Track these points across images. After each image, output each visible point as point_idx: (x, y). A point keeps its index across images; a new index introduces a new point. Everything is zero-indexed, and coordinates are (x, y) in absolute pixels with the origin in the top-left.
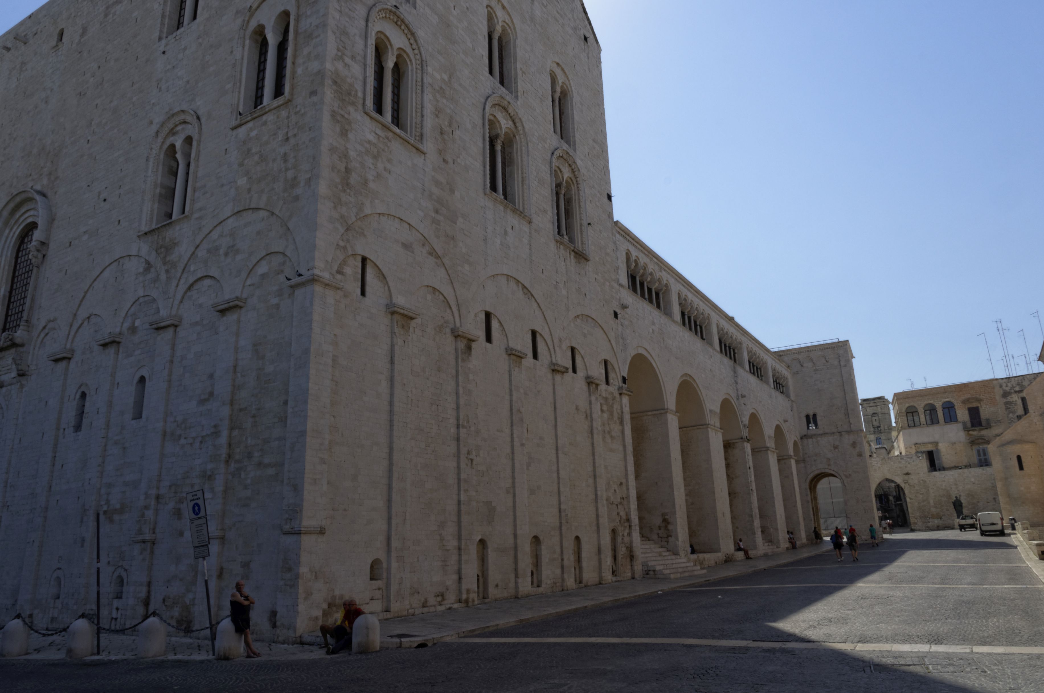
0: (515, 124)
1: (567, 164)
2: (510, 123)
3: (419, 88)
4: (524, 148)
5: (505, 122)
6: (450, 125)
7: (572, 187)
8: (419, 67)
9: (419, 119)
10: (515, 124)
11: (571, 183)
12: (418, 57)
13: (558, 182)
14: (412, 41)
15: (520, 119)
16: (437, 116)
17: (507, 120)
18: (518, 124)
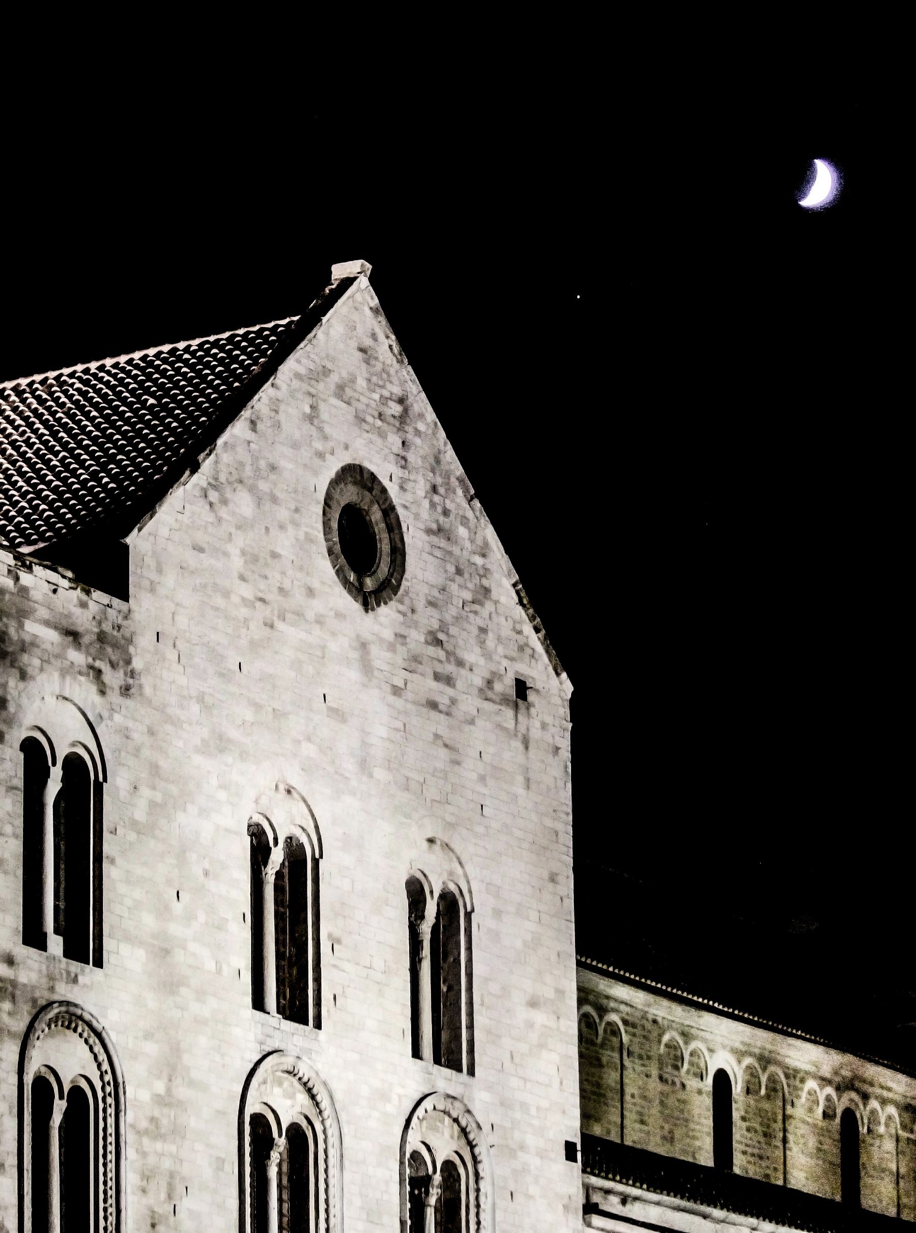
0: (313, 1097)
1: (447, 1120)
2: (303, 1098)
3: (111, 1148)
4: (331, 1152)
5: (289, 1102)
6: (170, 1197)
7: (461, 1171)
8: (110, 1100)
9: (112, 1219)
10: (313, 1097)
11: (458, 1161)
12: (108, 1077)
13: (422, 1173)
14: (98, 1048)
15: (325, 1084)
16: (144, 1191)
17: (292, 1096)
18: (319, 1098)
